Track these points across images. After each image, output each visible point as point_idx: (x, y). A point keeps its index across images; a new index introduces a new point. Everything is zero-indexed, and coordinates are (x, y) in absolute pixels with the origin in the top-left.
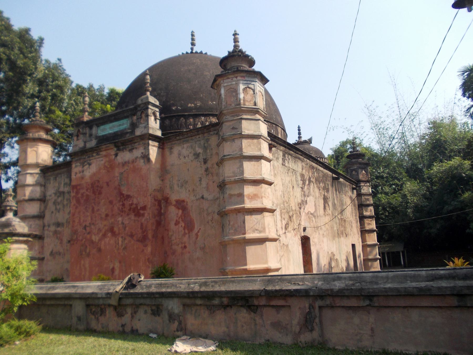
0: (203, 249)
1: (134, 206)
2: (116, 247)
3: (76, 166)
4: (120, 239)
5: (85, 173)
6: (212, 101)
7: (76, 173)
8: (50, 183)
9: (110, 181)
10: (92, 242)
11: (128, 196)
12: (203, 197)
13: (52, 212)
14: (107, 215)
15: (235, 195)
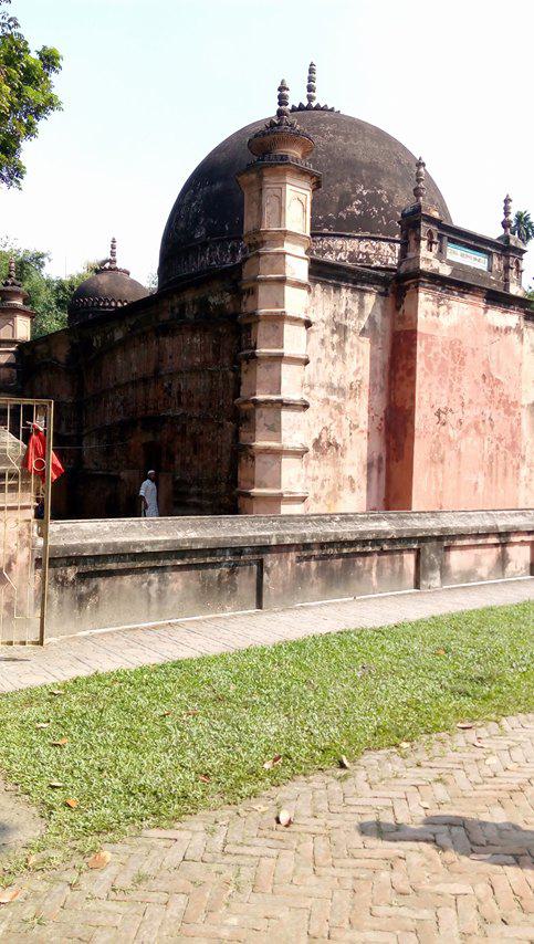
1: (504, 398)
3: (428, 300)
11: (498, 382)
14: (470, 402)
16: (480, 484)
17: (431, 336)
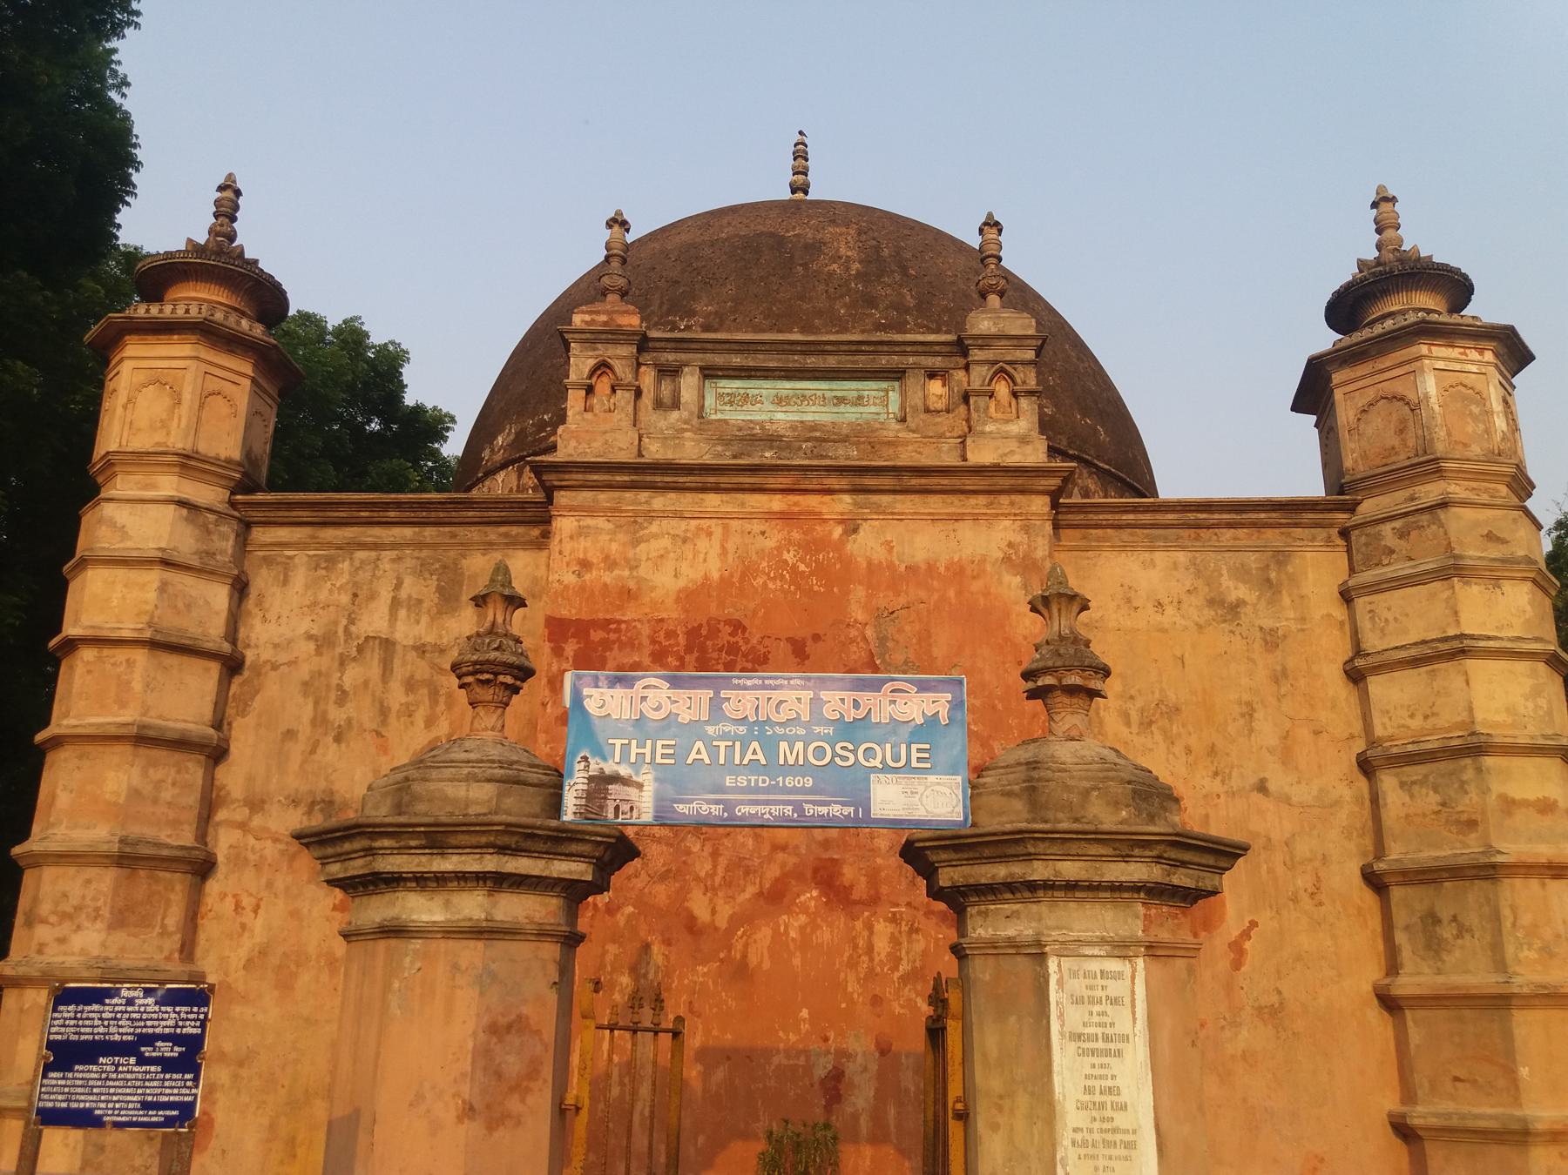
0: (1273, 1014)
2: (853, 964)
3: (581, 532)
4: (882, 928)
5: (643, 571)
6: (1084, 416)
7: (585, 565)
8: (285, 582)
9: (816, 638)
10: (692, 926)
12: (1262, 787)
13: (290, 734)
15: (1525, 803)
16: (851, 1069)
17: (605, 624)
